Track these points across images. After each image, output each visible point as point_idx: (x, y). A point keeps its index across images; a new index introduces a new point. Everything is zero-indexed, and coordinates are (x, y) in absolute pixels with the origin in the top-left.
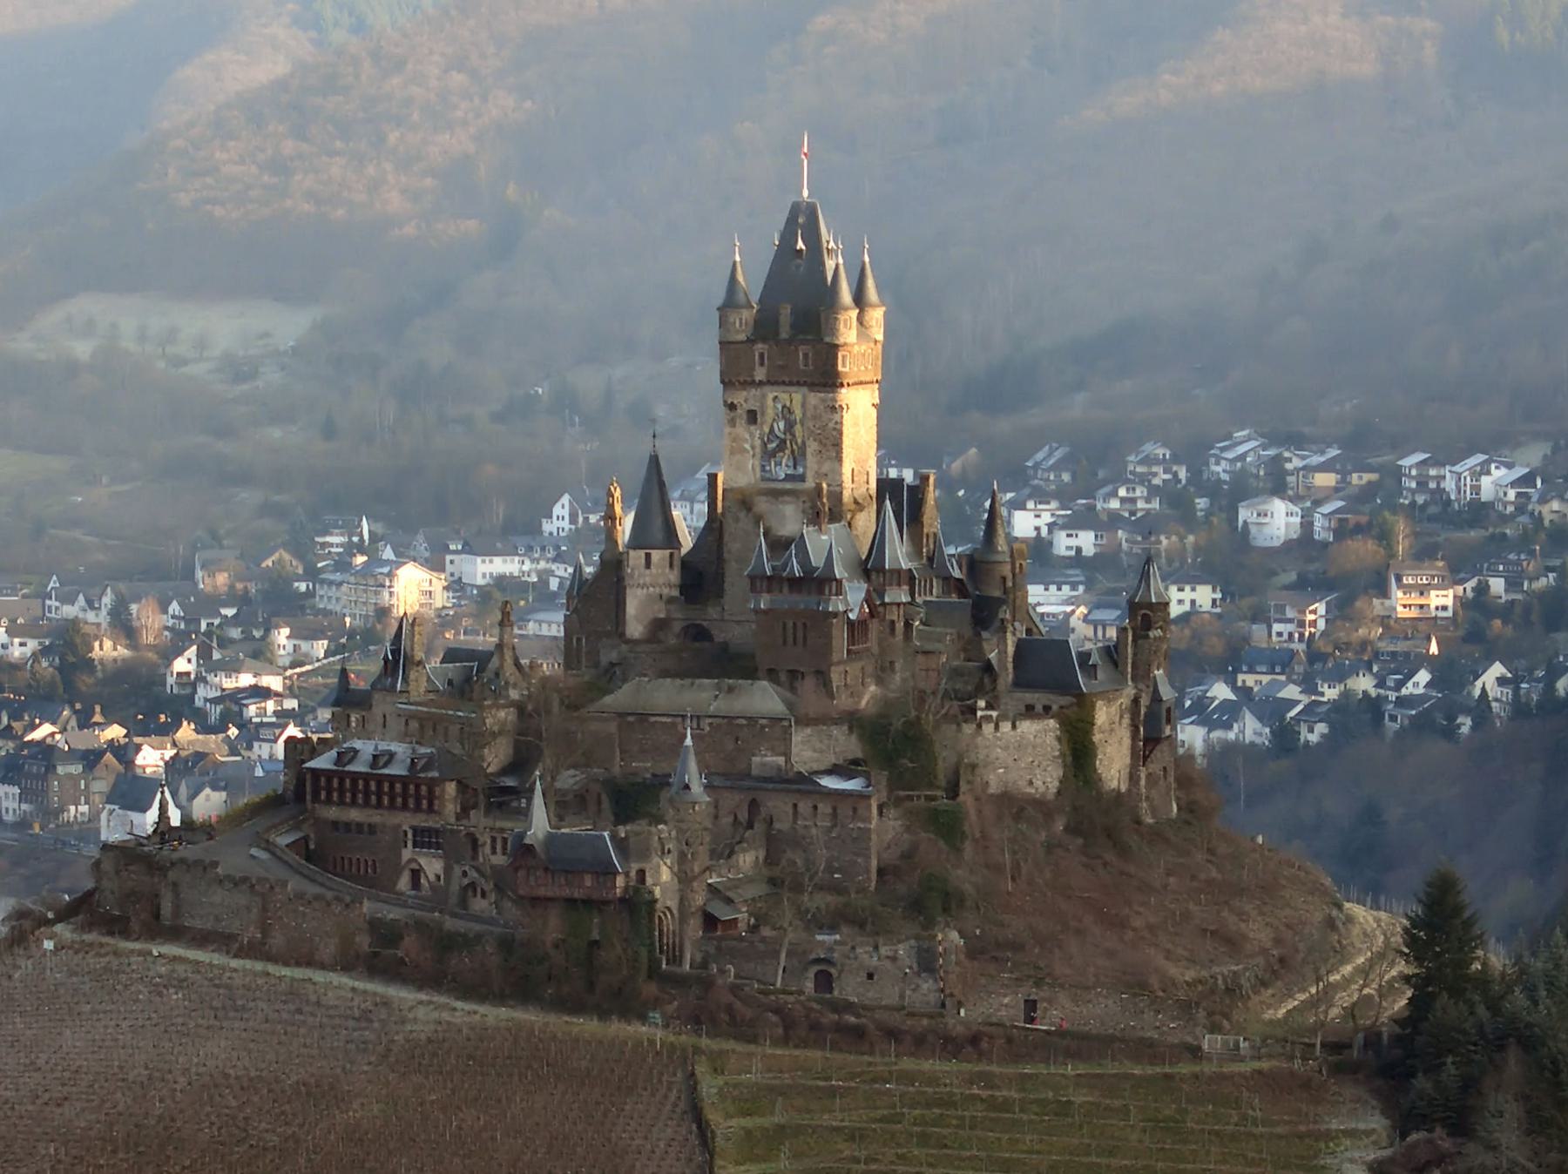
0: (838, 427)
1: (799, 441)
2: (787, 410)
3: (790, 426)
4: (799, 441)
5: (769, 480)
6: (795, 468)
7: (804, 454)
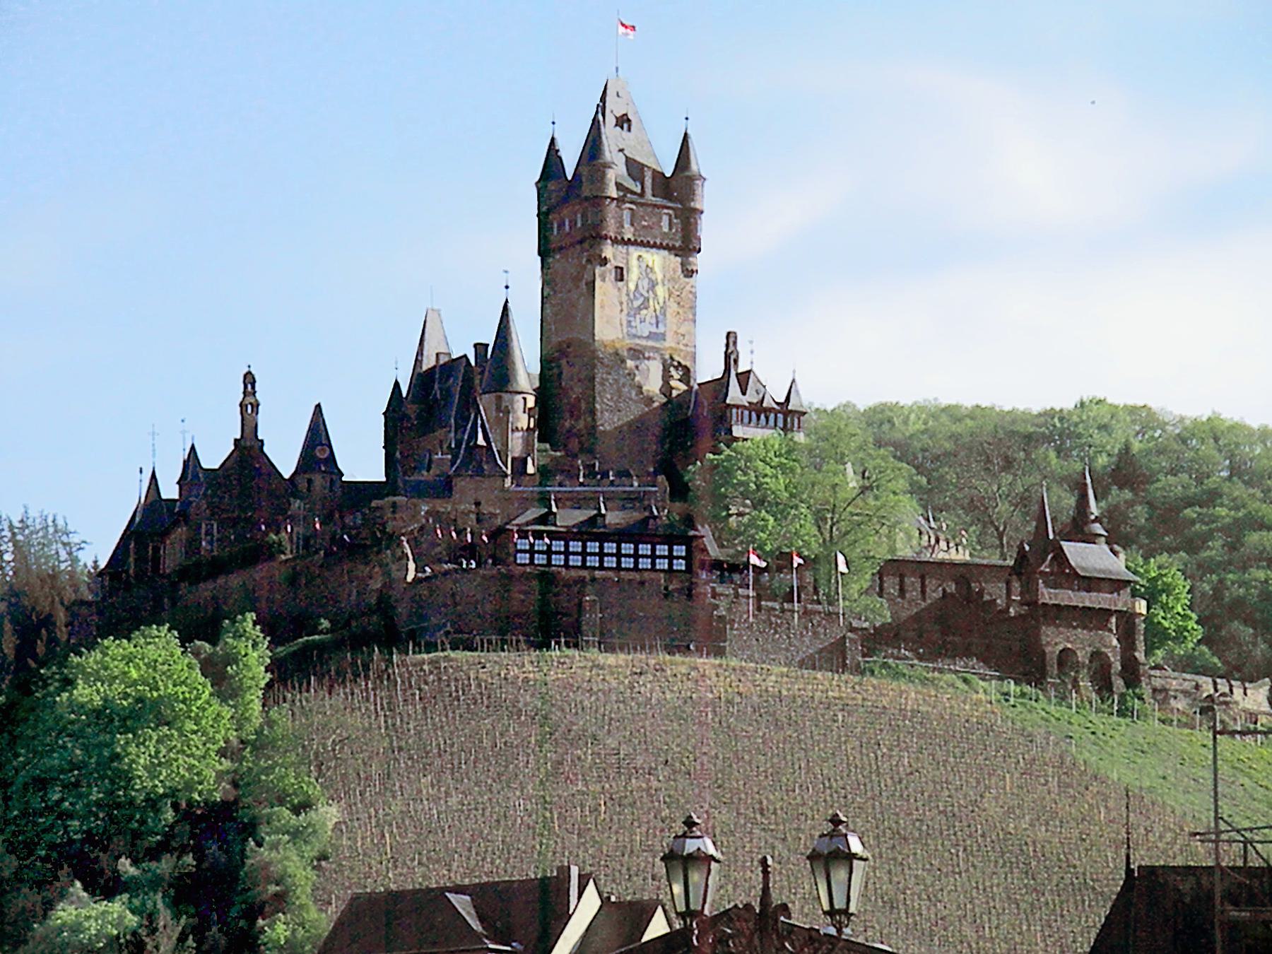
0: (693, 290)
1: (661, 301)
3: (653, 285)
4: (661, 301)
5: (635, 336)
6: (657, 326)
7: (665, 315)
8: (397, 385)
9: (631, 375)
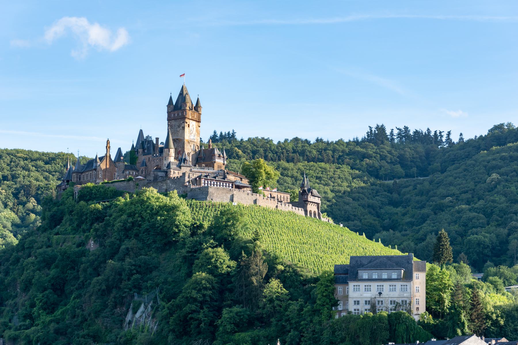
2: (193, 125)
8: (133, 145)
9: (191, 146)
